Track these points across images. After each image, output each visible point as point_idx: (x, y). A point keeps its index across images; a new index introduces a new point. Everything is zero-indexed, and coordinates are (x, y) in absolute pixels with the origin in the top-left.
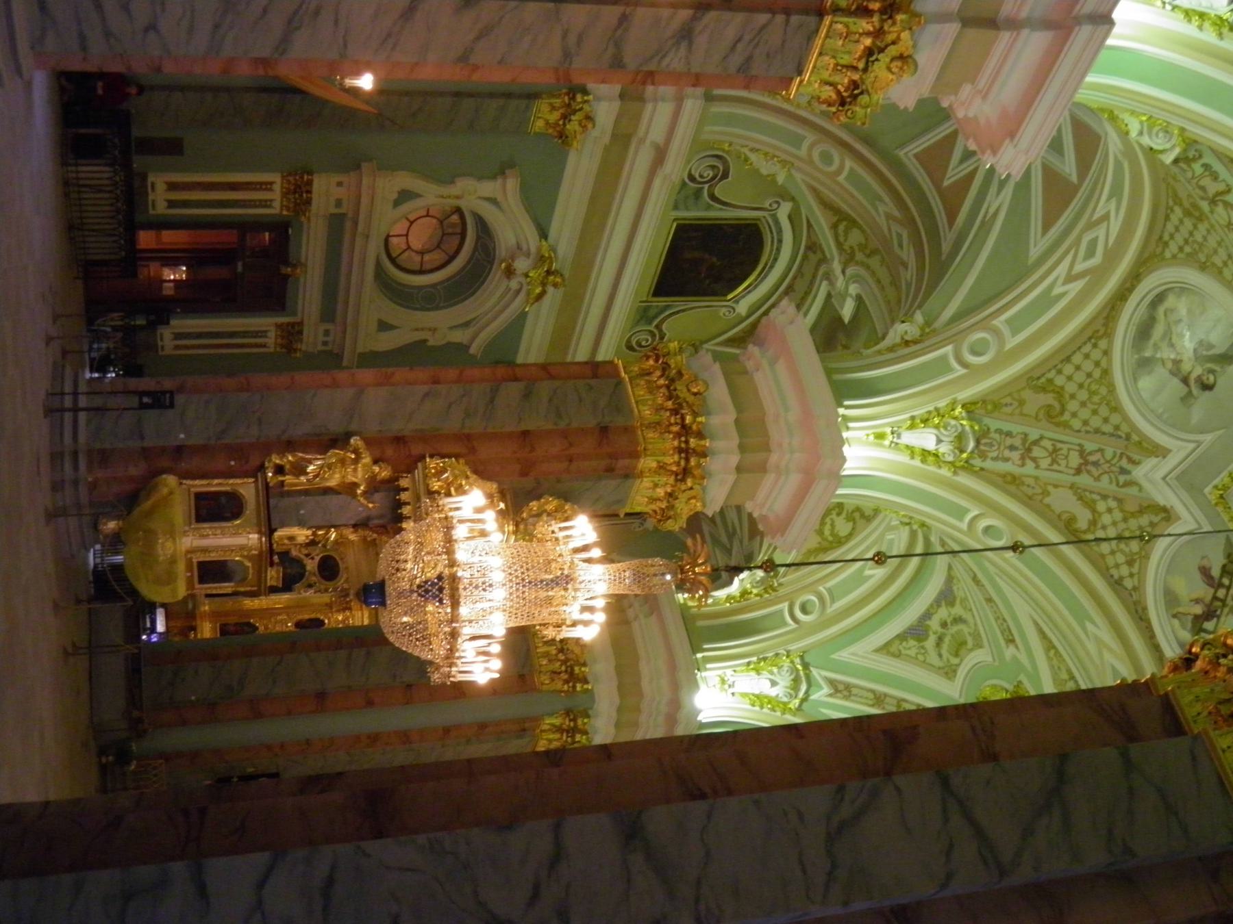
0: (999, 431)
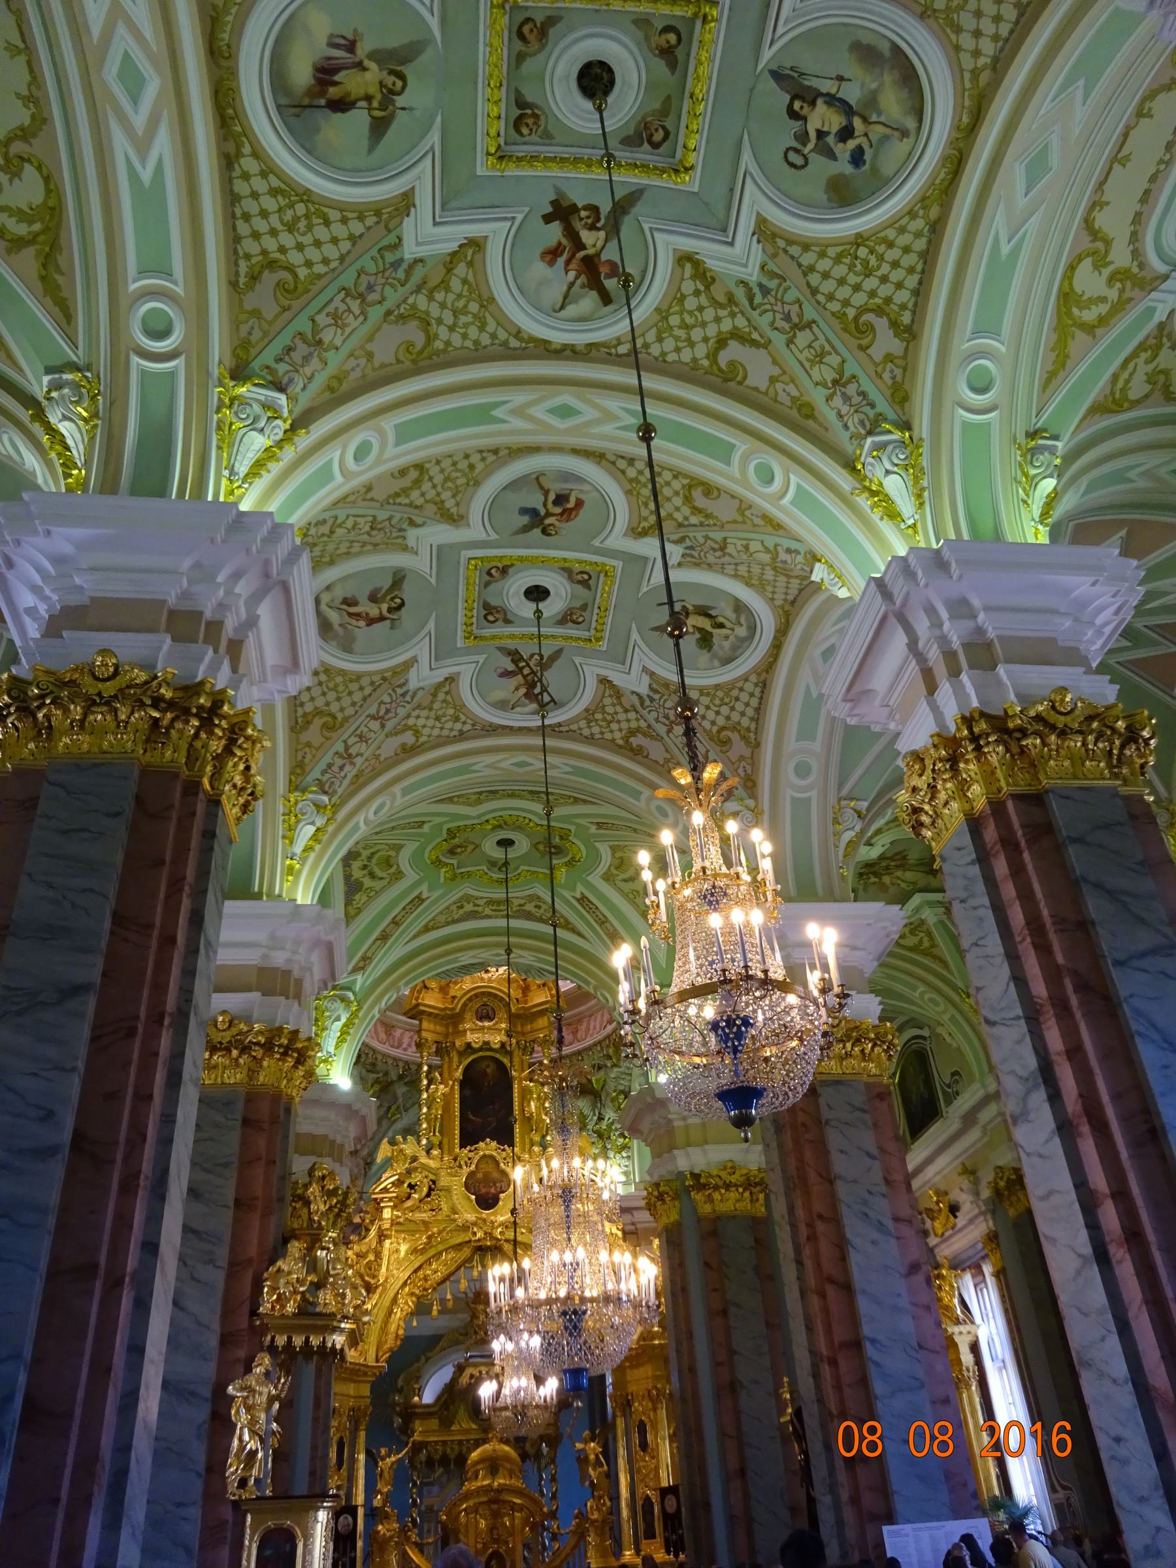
0: (324, 772)
